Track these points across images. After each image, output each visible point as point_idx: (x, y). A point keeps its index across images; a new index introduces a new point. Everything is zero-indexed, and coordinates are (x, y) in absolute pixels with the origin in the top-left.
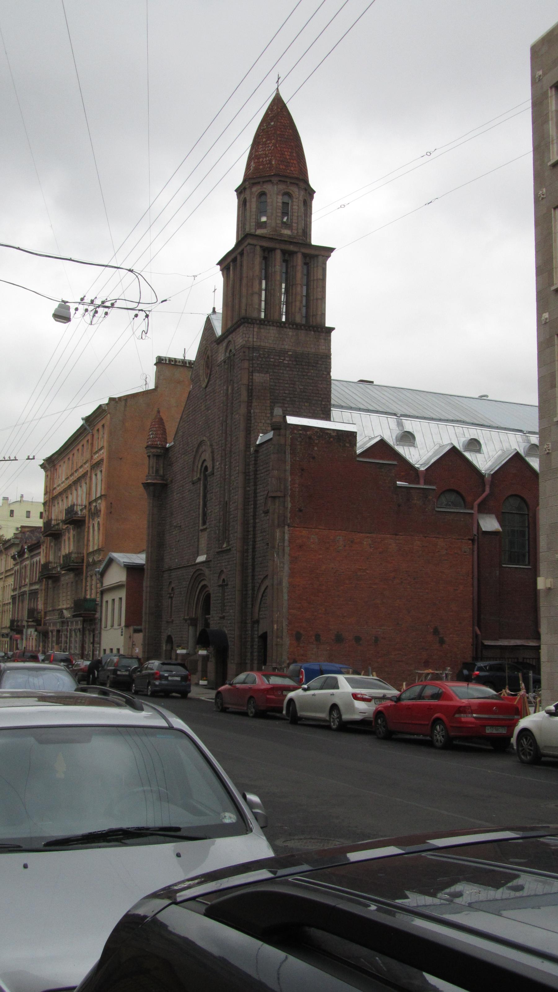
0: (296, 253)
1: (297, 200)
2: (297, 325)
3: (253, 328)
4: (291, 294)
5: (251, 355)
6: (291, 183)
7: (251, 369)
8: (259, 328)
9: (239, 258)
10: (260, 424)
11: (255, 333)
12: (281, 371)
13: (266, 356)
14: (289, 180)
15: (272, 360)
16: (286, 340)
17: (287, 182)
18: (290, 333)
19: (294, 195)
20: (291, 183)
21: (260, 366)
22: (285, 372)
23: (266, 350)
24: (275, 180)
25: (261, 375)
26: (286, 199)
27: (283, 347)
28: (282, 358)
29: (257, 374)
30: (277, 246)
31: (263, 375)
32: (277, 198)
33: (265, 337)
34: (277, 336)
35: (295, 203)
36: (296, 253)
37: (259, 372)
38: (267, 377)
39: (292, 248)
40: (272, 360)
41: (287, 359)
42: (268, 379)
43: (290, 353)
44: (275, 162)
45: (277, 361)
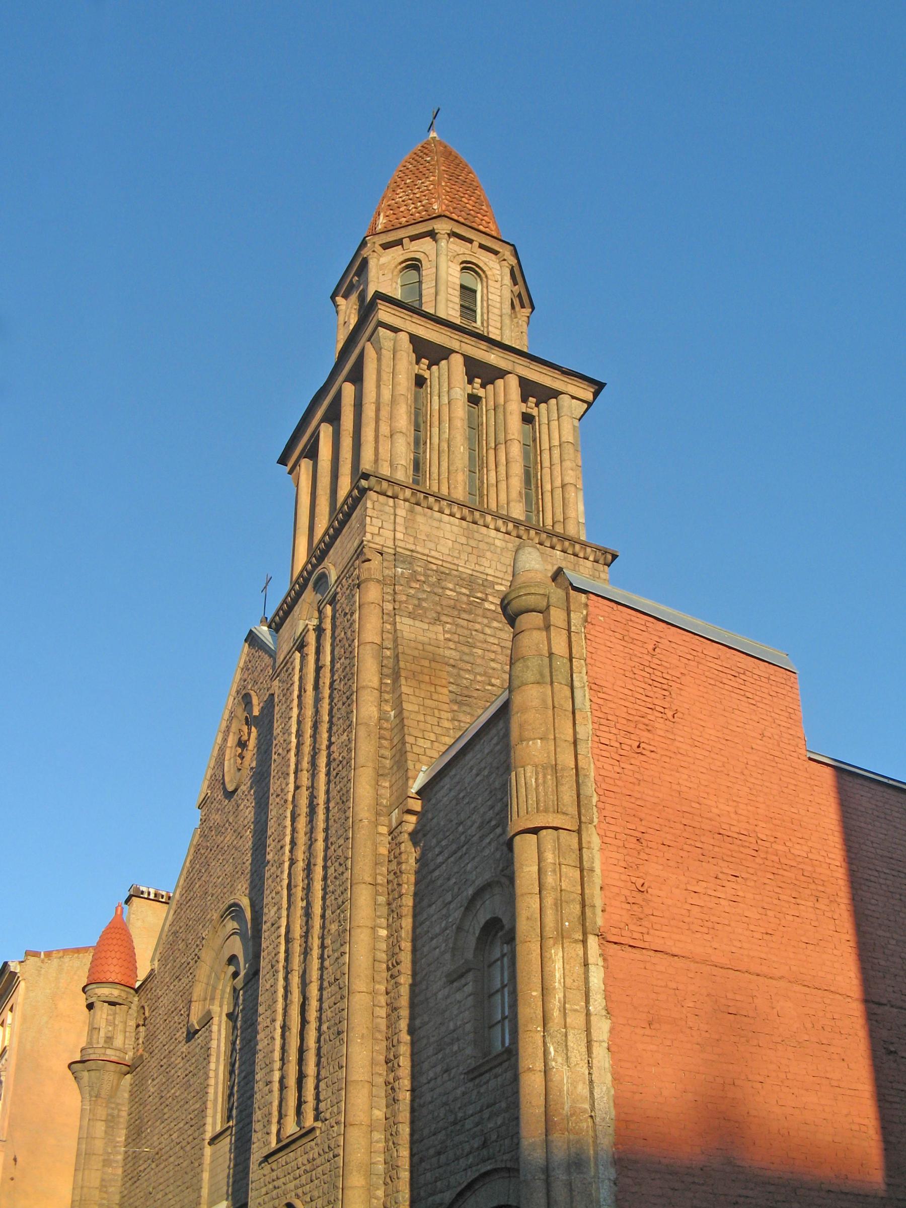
0: (502, 374)
1: (498, 285)
2: (517, 523)
3: (395, 507)
4: (492, 465)
5: (387, 572)
6: (481, 246)
7: (389, 607)
8: (411, 511)
9: (349, 390)
10: (421, 742)
11: (399, 520)
12: (478, 627)
13: (434, 579)
14: (479, 239)
15: (448, 593)
16: (488, 554)
17: (470, 241)
18: (498, 543)
19: (488, 273)
20: (481, 246)
21: (416, 602)
22: (488, 631)
23: (434, 567)
24: (443, 227)
25: (418, 623)
26: (470, 280)
27: (477, 568)
28: (479, 595)
29: (407, 620)
30: (454, 345)
31: (426, 626)
32: (448, 267)
33: (427, 536)
34: (463, 540)
35: (491, 289)
36: (502, 374)
37: (412, 616)
38: (438, 633)
39: (494, 358)
40: (448, 593)
41: (491, 598)
42: (441, 637)
43: (497, 587)
44: (440, 205)
45: (465, 599)
